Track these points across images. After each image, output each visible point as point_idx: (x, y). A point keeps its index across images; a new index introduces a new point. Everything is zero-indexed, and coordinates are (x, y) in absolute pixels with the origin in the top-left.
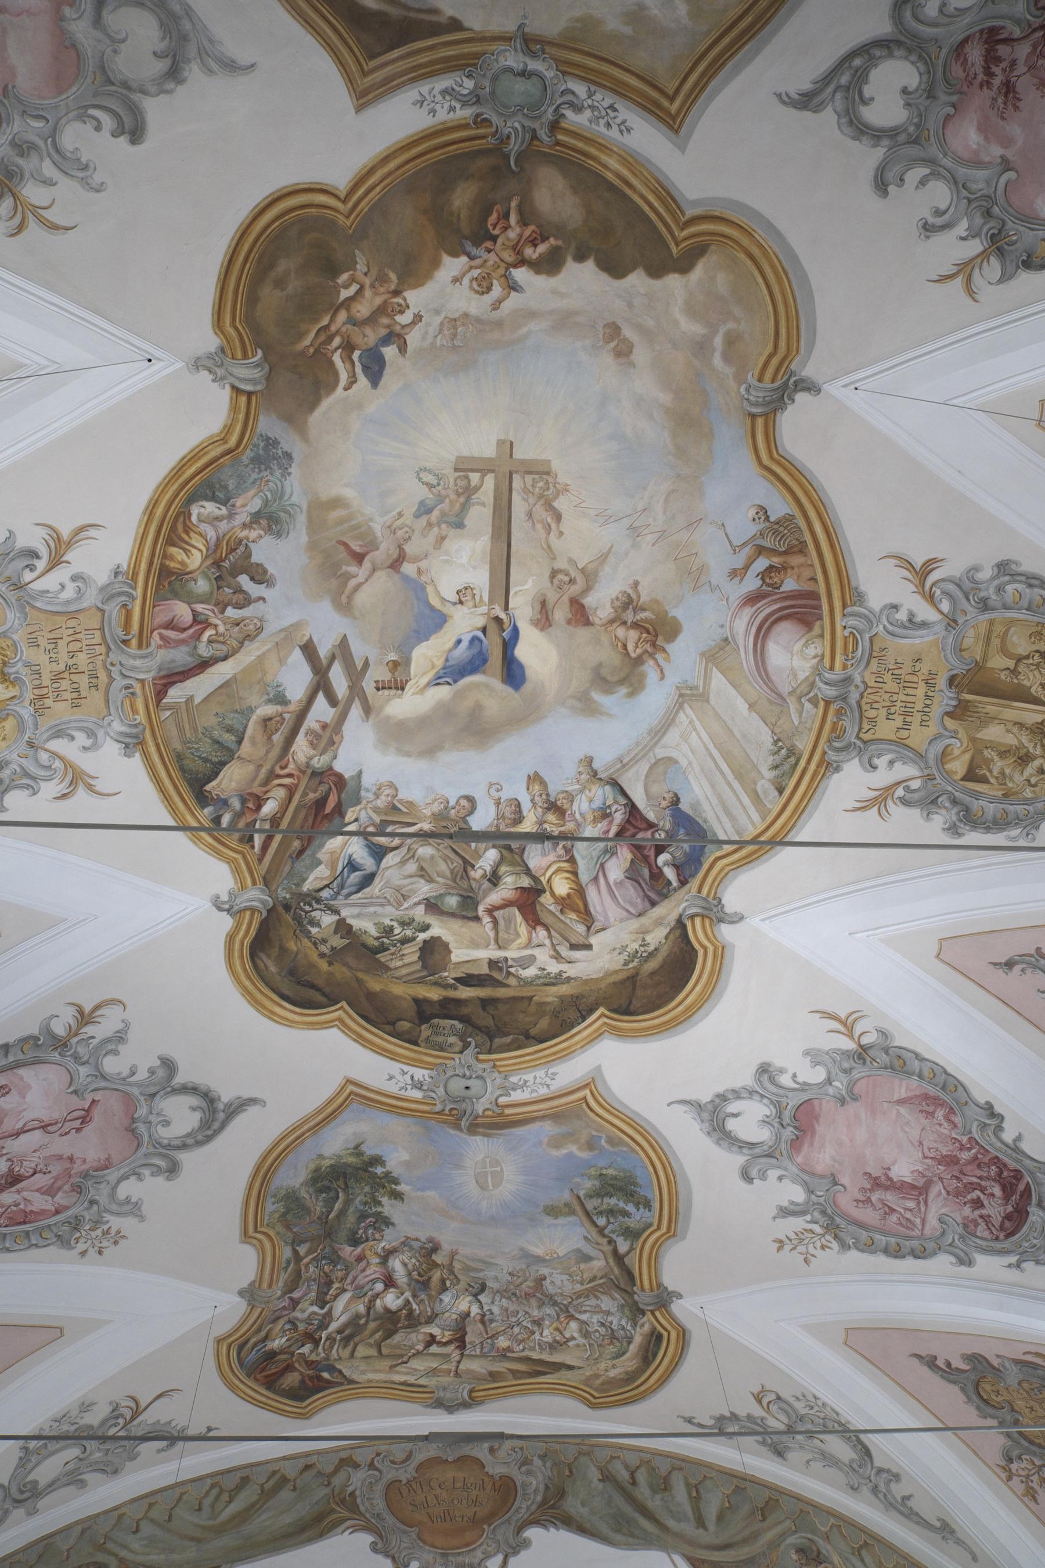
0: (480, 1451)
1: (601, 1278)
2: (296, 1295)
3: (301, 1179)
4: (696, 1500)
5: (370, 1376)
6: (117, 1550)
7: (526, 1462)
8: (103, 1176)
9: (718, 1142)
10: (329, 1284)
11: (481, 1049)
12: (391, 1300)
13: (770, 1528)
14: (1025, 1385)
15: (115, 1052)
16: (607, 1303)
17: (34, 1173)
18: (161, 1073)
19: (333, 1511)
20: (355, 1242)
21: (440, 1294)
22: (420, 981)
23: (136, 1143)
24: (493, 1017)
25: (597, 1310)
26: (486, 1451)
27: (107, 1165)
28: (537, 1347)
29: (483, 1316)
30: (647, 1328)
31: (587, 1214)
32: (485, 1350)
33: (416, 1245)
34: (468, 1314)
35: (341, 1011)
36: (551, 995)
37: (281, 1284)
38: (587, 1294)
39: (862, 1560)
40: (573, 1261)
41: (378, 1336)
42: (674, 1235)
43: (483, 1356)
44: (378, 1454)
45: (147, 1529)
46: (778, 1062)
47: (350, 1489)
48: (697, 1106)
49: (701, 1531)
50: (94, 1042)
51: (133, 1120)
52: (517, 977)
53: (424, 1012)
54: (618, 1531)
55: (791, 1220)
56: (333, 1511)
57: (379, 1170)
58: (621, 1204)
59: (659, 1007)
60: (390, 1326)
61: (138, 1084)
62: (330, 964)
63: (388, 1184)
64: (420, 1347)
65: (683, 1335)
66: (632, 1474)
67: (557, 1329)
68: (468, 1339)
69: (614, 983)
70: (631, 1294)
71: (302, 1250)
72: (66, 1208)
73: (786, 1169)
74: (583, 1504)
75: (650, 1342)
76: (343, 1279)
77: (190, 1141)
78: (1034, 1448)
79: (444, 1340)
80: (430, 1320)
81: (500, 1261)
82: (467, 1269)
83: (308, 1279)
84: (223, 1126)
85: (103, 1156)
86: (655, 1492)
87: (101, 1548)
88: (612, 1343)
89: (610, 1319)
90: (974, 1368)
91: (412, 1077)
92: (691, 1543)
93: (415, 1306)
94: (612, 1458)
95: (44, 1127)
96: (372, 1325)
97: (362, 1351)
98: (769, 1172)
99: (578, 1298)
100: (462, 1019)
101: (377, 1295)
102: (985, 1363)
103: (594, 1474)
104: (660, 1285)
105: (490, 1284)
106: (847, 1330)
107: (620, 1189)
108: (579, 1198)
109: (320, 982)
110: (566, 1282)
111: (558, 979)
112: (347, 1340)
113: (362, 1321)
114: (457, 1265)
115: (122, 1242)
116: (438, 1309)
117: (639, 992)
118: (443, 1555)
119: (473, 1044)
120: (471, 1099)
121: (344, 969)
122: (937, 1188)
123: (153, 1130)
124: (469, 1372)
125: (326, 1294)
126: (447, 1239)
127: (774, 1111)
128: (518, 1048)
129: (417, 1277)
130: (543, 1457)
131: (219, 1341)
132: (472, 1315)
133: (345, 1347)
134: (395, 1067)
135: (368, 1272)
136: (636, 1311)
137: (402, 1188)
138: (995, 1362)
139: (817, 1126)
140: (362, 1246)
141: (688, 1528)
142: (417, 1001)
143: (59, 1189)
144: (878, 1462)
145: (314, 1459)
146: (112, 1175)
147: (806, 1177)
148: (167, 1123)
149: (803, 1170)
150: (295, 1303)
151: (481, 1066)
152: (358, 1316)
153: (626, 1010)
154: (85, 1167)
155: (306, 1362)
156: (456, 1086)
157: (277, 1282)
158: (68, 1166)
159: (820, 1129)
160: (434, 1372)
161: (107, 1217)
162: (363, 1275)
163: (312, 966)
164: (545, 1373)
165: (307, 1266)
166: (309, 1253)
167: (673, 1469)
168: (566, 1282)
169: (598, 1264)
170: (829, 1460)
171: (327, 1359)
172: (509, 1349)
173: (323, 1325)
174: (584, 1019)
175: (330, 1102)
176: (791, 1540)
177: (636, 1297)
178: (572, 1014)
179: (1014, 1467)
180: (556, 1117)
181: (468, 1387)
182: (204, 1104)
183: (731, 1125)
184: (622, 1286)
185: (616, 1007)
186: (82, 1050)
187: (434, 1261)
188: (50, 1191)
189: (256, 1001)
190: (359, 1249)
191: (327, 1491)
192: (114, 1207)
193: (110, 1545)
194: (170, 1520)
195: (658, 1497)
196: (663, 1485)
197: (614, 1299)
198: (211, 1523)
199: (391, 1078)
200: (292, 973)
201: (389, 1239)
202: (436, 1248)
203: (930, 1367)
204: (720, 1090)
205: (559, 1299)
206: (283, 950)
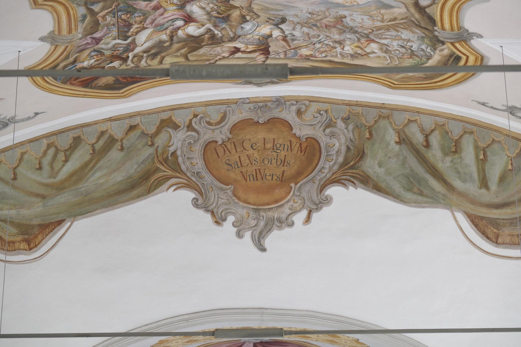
0: (290, 116)
1: (402, 19)
2: (97, 35)
7: (330, 124)
10: (130, 26)
12: (192, 30)
16: (405, 34)
19: (157, 170)
21: (241, 24)
26: (294, 114)
28: (339, 55)
30: (446, 52)
34: (270, 36)
37: (80, 30)
40: (373, 8)
44: (195, 116)
47: (172, 149)
49: (484, 191)
54: (410, 190)
56: (157, 170)
64: (226, 55)
66: (427, 137)
68: (271, 49)
70: (432, 31)
71: (96, 8)
74: (380, 165)
75: (448, 60)
82: (266, 9)
83: (108, 25)
86: (446, 152)
89: (409, 44)
92: (473, 202)
94: (410, 121)
96: (176, 46)
101: (179, 28)
103: (392, 137)
116: (239, 32)
118: (256, 210)
125: (128, 32)
129: (217, 15)
130: (346, 120)
132: (274, 36)
135: (166, 15)
145: (137, 120)
150: (98, 41)
152: (161, 42)
157: (76, 29)
162: (162, 17)
165: (104, 17)
166: (102, 9)
167: (465, 132)
172: (311, 55)
177: (436, 33)
184: (423, 26)
187: (231, 5)
191: (151, 150)
194: (15, 179)
195: (448, 159)
197: (413, 32)
198: (51, 181)
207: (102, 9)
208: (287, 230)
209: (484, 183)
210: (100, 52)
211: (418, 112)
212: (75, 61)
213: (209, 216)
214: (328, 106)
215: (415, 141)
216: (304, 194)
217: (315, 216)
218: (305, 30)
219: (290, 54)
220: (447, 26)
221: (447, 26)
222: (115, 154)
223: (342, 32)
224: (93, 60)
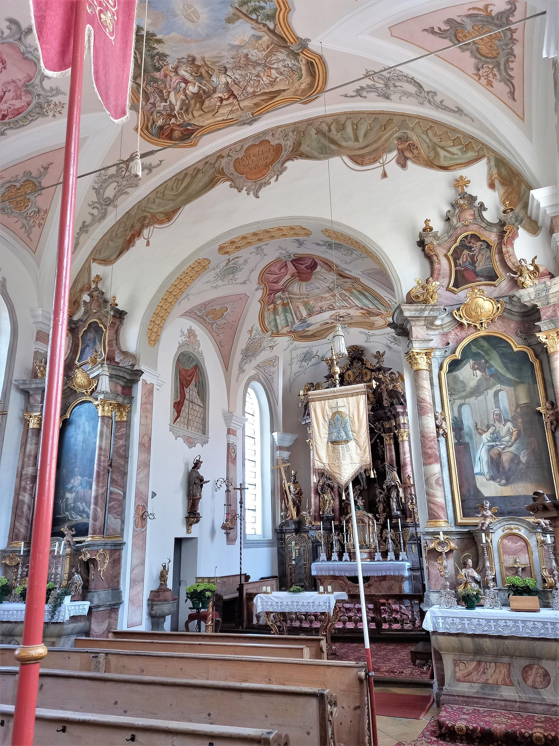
4: (355, 130)
5: (207, 122)
7: (287, 135)
8: (33, 83)
10: (161, 91)
12: (192, 89)
13: (387, 133)
14: (476, 28)
17: (5, 93)
20: (158, 70)
23: (33, 64)
25: (279, 61)
29: (234, 81)
30: (304, 61)
32: (246, 96)
33: (185, 60)
39: (427, 135)
41: (198, 105)
42: (290, 10)
43: (246, 98)
45: (157, 201)
47: (221, 167)
49: (356, 143)
51: (23, 54)
54: (322, 153)
60: (200, 100)
61: (10, 36)
65: (321, 58)
67: (268, 76)
70: (288, 47)
72: (31, 102)
75: (309, 67)
76: (165, 87)
78: (488, 60)
79: (226, 97)
80: (215, 91)
81: (224, 54)
82: (214, 63)
85: (26, 75)
86: (338, 131)
87: (144, 211)
88: (294, 74)
89: (286, 63)
90: (451, 27)
92: (351, 149)
93: (204, 88)
96: (192, 102)
97: (196, 114)
99: (267, 58)
101: (185, 89)
102: (454, 22)
103: (313, 132)
104: (298, 38)
105: (227, 66)
110: (257, 53)
112: (187, 111)
113: (187, 102)
116: (214, 85)
124: (246, 107)
125: (164, 96)
132: (230, 82)
133: (188, 114)
135: (174, 80)
136: (295, 55)
137: (159, 37)
138: (459, 20)
140: (162, 70)
141: (351, 144)
144: (426, 90)
150: (154, 104)
152: (183, 101)
154: (22, 83)
155: (177, 125)
158: (15, 85)
160: (231, 112)
161: (50, 99)
162: (172, 82)
164: (276, 97)
167: (347, 119)
168: (257, 53)
170: (407, 94)
171: (185, 121)
172: (254, 92)
173: (173, 109)
179: (480, 72)
181: (250, 113)
191: (214, 170)
193: (147, 209)
196: (342, 128)
197: (282, 53)
198: (176, 193)
201: (171, 63)
202: (194, 59)
203: (433, 34)
205: (260, 62)
208: (268, 186)
209: (357, 139)
212: (154, 122)
213: (236, 190)
214: (283, 128)
215: (324, 131)
216: (275, 169)
217: (280, 177)
222: (200, 175)
224: (161, 120)
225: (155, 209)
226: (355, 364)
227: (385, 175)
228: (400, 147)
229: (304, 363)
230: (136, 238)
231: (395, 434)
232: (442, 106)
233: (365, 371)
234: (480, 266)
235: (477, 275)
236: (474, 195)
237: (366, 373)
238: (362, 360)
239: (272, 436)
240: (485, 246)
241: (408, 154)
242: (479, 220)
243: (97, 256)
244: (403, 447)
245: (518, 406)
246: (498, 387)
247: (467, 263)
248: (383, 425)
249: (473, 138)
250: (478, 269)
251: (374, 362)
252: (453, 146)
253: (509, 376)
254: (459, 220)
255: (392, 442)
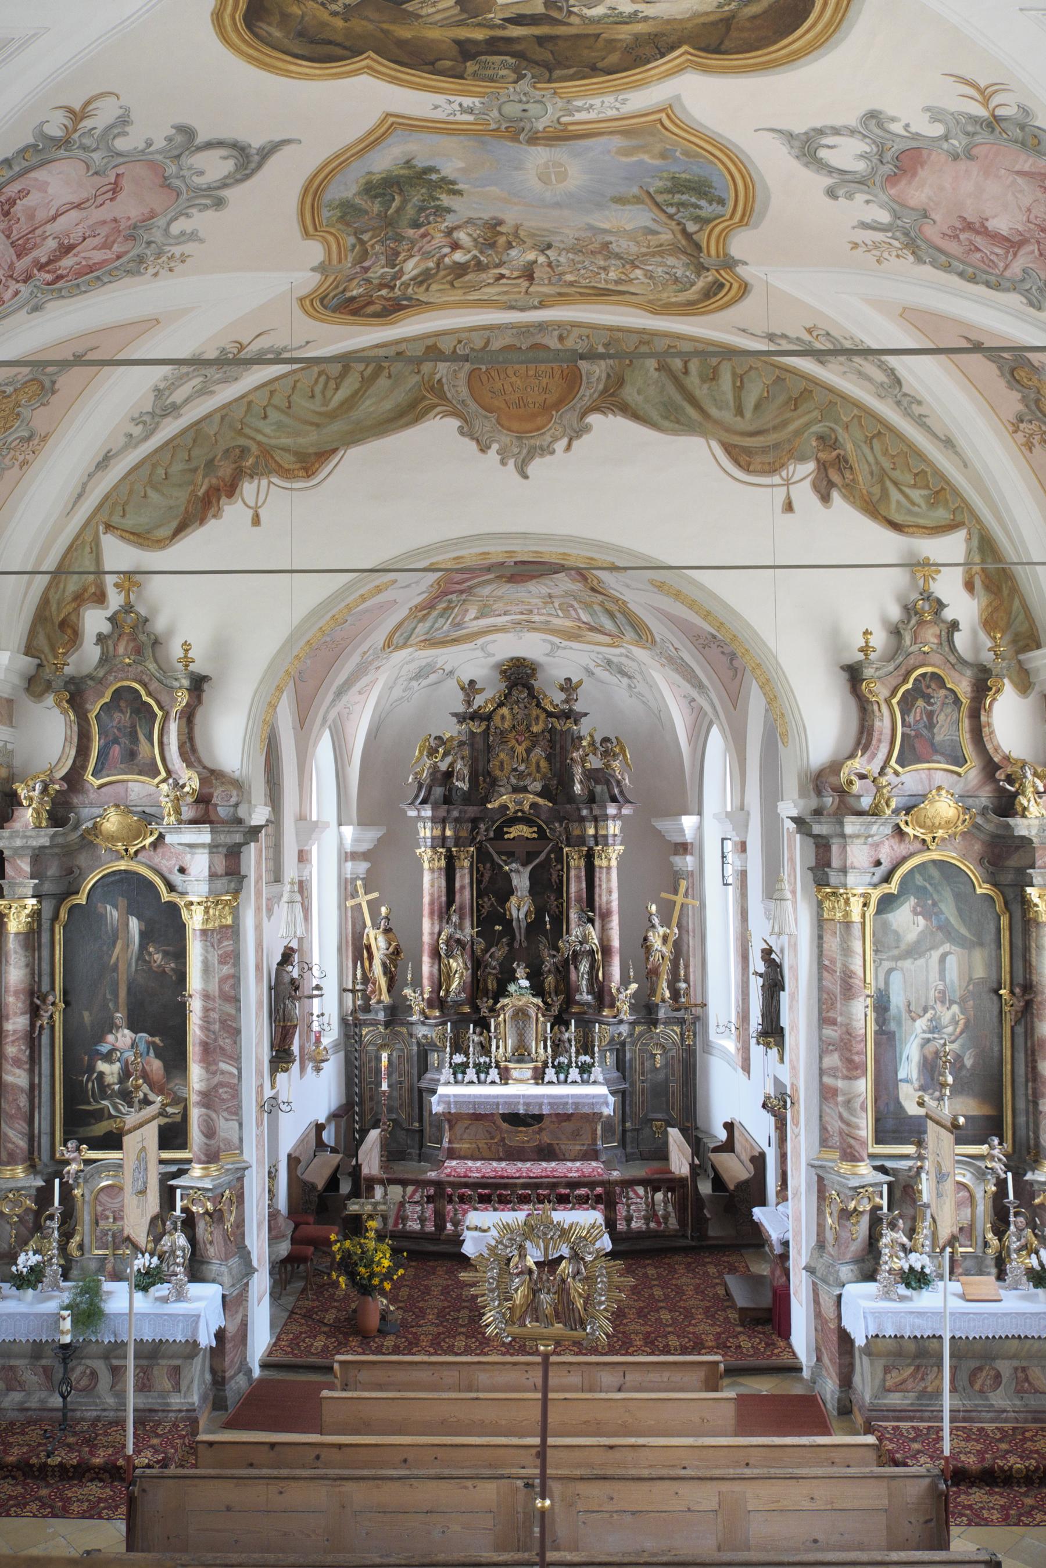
2: (366, 264)
3: (354, 191)
4: (739, 389)
6: (252, 434)
9: (806, 165)
10: (398, 254)
11: (537, 79)
12: (459, 257)
13: (799, 417)
15: (125, 134)
16: (671, 261)
17: (84, 239)
18: (179, 139)
19: (424, 398)
20: (416, 225)
22: (460, 24)
24: (552, 52)
26: (556, 340)
27: (153, 215)
30: (710, 279)
31: (657, 205)
33: (479, 222)
34: (536, 262)
35: (370, 58)
36: (624, 33)
37: (350, 259)
38: (653, 254)
39: (872, 448)
43: (550, 283)
44: (460, 342)
45: (274, 415)
46: (891, 112)
47: (437, 377)
48: (789, 136)
49: (739, 418)
50: (97, 132)
51: (165, 178)
52: (582, 17)
53: (466, 51)
54: (666, 418)
55: (870, 232)
56: (424, 398)
57: (434, 177)
58: (693, 200)
59: (757, 49)
62: (346, 20)
63: (448, 185)
69: (704, 24)
71: (365, 237)
73: (876, 196)
74: (639, 393)
77: (228, 181)
82: (533, 235)
83: (376, 254)
84: (259, 166)
85: (146, 211)
86: (704, 379)
87: (240, 432)
91: (461, 105)
92: (728, 430)
95: (78, 206)
96: (442, 273)
97: (434, 287)
98: (857, 195)
100: (513, 55)
104: (726, 255)
106: (905, 309)
107: (694, 189)
108: (648, 193)
109: (339, 38)
111: (633, 18)
112: (421, 283)
114: (522, 233)
115: (188, 260)
116: (505, 258)
117: (734, 34)
118: (519, 438)
119: (529, 75)
120: (529, 119)
121: (364, 23)
122: (1028, 248)
123: (188, 181)
126: (511, 216)
127: (875, 150)
128: (584, 78)
131: (301, 300)
134: (440, 99)
136: (701, 269)
137: (459, 187)
139: (919, 170)
141: (727, 416)
142: (458, 42)
143: (114, 242)
144: (905, 389)
146: (161, 221)
147: (896, 207)
148: (201, 173)
149: (894, 201)
150: (366, 270)
151: (537, 92)
152: (428, 269)
153: (717, 49)
156: (512, 110)
159: (922, 173)
160: (506, 293)
163: (324, 25)
165: (373, 246)
166: (371, 239)
169: (666, 237)
173: (396, 277)
174: (663, 55)
175: (370, 133)
176: (815, 429)
178: (648, 50)
179: (1022, 426)
180: (626, 133)
182: (235, 153)
183: (822, 153)
185: (703, 45)
186: (86, 141)
188: (106, 246)
189: (266, 64)
190: (422, 230)
192: (172, 241)
193: (247, 431)
194: (289, 407)
195: (706, 386)
196: (712, 376)
198: (323, 409)
199: (436, 107)
200: (301, 34)
201: (450, 221)
204: (818, 125)
206: (285, 18)
207: (371, 239)
208: (548, 458)
209: (739, 411)
210: (368, 281)
211: (679, 337)
212: (344, 290)
213: (474, 444)
215: (674, 368)
216: (565, 422)
217: (576, 444)
218: (571, 256)
219: (554, 280)
220: (713, 252)
221: (713, 252)
222: (383, 382)
223: (607, 258)
225: (268, 432)
226: (515, 692)
227: (789, 507)
228: (822, 456)
229: (414, 683)
230: (224, 500)
231: (591, 849)
232: (920, 421)
233: (535, 712)
234: (942, 734)
235: (936, 751)
236: (945, 602)
237: (537, 718)
238: (530, 689)
239: (340, 833)
240: (950, 700)
241: (835, 477)
242: (947, 649)
243: (116, 520)
244: (609, 880)
245: (971, 979)
246: (947, 947)
247: (921, 725)
248: (567, 829)
249: (948, 482)
250: (938, 738)
251: (558, 697)
252: (914, 486)
253: (964, 931)
254: (915, 639)
255: (582, 863)
